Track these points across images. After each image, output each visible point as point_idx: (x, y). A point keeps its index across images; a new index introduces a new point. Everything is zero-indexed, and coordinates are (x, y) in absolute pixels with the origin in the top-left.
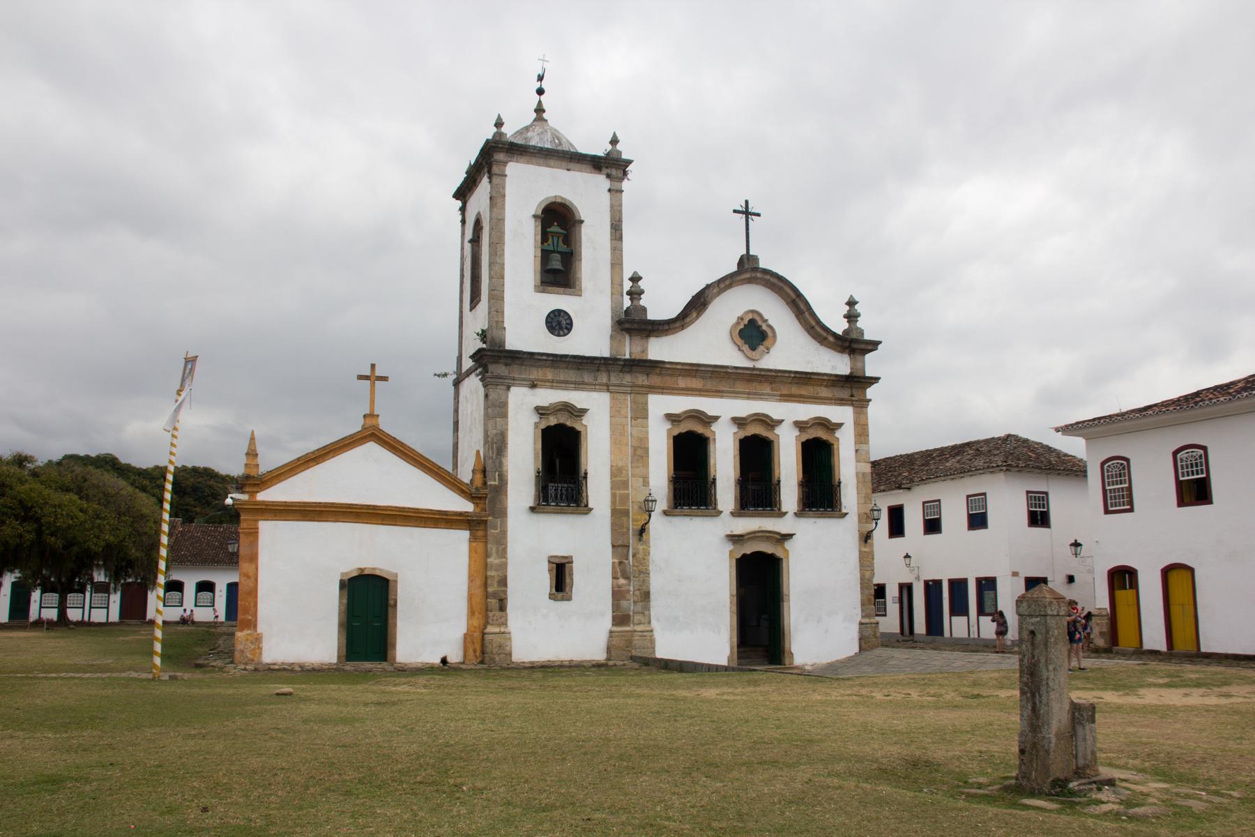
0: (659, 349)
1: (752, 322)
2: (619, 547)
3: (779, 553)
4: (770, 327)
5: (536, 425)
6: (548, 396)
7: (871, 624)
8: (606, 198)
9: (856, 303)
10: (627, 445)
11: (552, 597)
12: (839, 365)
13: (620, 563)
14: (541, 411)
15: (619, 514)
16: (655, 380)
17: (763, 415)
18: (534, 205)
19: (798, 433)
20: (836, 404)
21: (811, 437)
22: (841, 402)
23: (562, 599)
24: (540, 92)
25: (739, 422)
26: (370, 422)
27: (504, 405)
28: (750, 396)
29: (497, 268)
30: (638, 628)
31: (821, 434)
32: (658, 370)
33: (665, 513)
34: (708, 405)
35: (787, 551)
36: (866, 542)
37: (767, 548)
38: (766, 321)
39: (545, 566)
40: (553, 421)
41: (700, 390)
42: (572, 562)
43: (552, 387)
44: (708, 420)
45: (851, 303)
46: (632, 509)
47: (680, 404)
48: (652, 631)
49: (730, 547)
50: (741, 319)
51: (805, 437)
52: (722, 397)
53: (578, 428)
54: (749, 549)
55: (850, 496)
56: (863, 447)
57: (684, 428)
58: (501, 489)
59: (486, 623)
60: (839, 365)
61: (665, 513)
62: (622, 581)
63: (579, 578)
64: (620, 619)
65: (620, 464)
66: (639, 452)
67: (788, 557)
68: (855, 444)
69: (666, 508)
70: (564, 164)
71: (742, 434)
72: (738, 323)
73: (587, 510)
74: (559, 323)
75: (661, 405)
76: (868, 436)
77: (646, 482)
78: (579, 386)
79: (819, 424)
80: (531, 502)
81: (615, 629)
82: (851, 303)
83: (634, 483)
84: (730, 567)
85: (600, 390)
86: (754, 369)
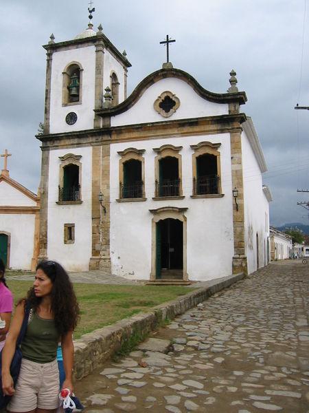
0: (116, 121)
1: (167, 98)
2: (95, 218)
3: (181, 219)
4: (177, 98)
5: (60, 165)
7: (239, 258)
8: (94, 55)
9: (235, 74)
10: (100, 169)
11: (65, 242)
13: (98, 226)
14: (62, 159)
16: (114, 137)
17: (169, 145)
18: (63, 68)
19: (194, 152)
20: (218, 133)
21: (201, 154)
22: (222, 131)
23: (70, 243)
24: (91, 17)
25: (157, 151)
26: (4, 173)
27: (48, 158)
28: (164, 136)
29: (48, 100)
30: (103, 257)
32: (114, 132)
33: (118, 201)
34: (138, 145)
35: (185, 218)
36: (237, 210)
37: (174, 216)
38: (174, 95)
40: (67, 163)
41: (137, 138)
42: (74, 227)
43: (67, 148)
45: (233, 74)
47: (123, 146)
48: (110, 259)
49: (152, 216)
50: (160, 97)
51: (198, 154)
52: (148, 139)
53: (77, 164)
54: (163, 217)
55: (226, 185)
56: (236, 155)
57: (128, 158)
60: (222, 110)
61: (118, 201)
62: (98, 234)
63: (77, 233)
64: (95, 252)
65: (96, 179)
66: (106, 172)
67: (186, 221)
68: (232, 153)
69: (118, 198)
70: (75, 47)
71: (160, 157)
72: (157, 100)
73: (81, 203)
74: (71, 118)
75: (116, 148)
76: (240, 148)
77: (108, 187)
78: (79, 145)
79: (207, 146)
81: (94, 257)
82: (233, 74)
83: (102, 188)
84: (152, 227)
85: (88, 146)
86: (166, 122)
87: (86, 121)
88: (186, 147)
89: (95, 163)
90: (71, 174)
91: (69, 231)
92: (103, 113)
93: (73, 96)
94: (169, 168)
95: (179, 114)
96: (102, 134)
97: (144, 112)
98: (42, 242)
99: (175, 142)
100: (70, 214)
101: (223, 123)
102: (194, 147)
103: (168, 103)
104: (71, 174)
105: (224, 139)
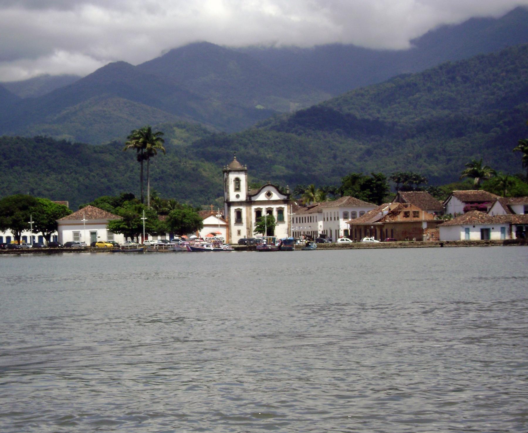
0: (253, 199)
2: (248, 228)
6: (236, 208)
12: (285, 197)
14: (236, 210)
15: (247, 223)
31: (281, 209)
34: (261, 207)
39: (237, 231)
44: (262, 209)
46: (250, 223)
57: (257, 210)
59: (229, 239)
60: (285, 197)
74: (238, 196)
75: (254, 207)
77: (251, 218)
80: (234, 222)
87: (243, 197)
89: (247, 211)
90: (239, 214)
91: (239, 232)
92: (249, 196)
96: (249, 202)
97: (262, 197)
99: (272, 206)
100: (239, 227)
101: (285, 202)
102: (277, 208)
103: (269, 194)
104: (239, 214)
105: (285, 207)
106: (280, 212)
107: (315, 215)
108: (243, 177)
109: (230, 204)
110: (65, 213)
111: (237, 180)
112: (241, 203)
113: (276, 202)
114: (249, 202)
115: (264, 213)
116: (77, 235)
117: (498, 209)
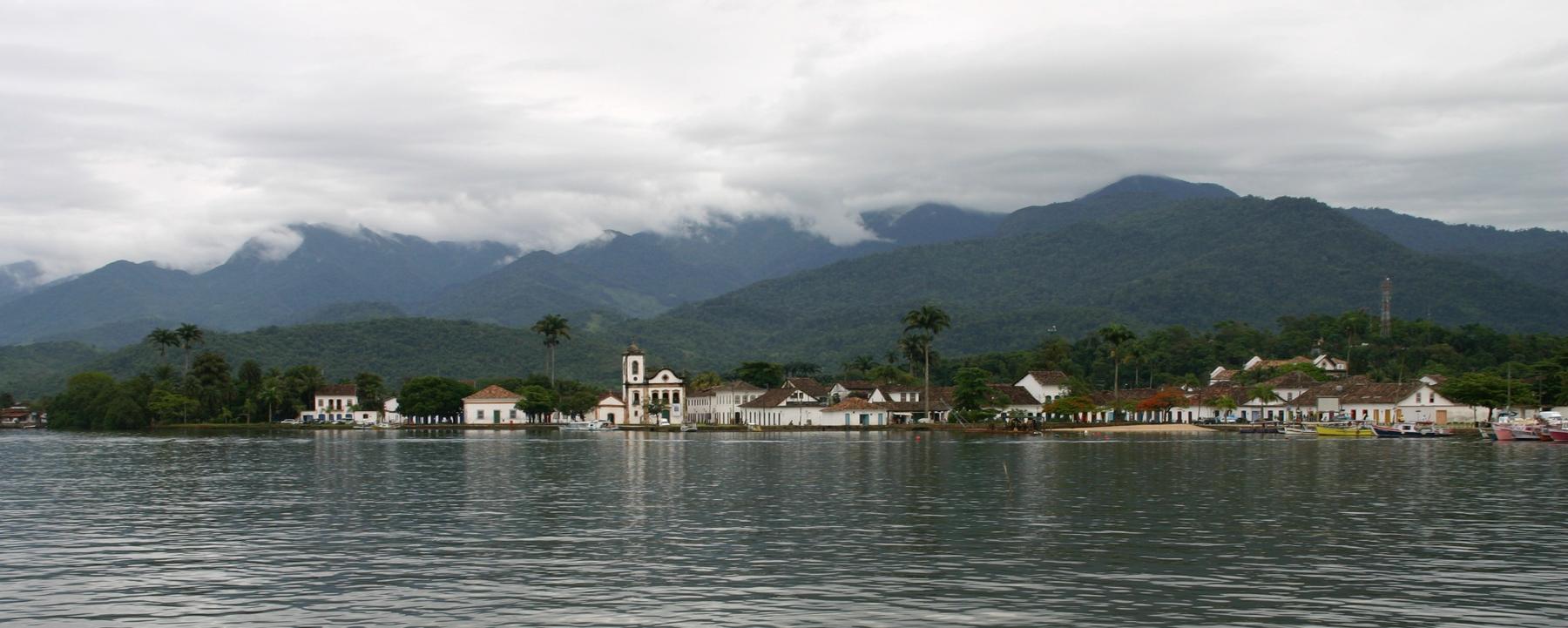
12: (681, 381)
34: (657, 389)
47: (653, 389)
58: (627, 402)
60: (681, 381)
74: (635, 379)
75: (651, 390)
87: (640, 380)
88: (671, 390)
91: (636, 413)
92: (646, 378)
93: (635, 371)
94: (666, 395)
95: (669, 381)
96: (646, 385)
97: (658, 379)
98: (627, 416)
101: (680, 385)
103: (665, 377)
104: (637, 396)
106: (676, 395)
107: (708, 398)
108: (640, 359)
109: (628, 385)
110: (469, 392)
111: (635, 364)
112: (639, 385)
113: (672, 385)
114: (646, 385)
115: (660, 396)
116: (481, 414)
117: (877, 397)
